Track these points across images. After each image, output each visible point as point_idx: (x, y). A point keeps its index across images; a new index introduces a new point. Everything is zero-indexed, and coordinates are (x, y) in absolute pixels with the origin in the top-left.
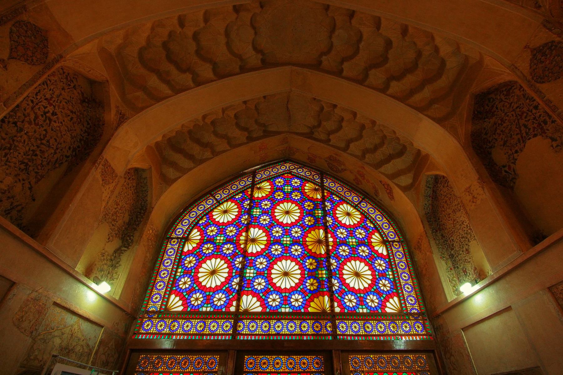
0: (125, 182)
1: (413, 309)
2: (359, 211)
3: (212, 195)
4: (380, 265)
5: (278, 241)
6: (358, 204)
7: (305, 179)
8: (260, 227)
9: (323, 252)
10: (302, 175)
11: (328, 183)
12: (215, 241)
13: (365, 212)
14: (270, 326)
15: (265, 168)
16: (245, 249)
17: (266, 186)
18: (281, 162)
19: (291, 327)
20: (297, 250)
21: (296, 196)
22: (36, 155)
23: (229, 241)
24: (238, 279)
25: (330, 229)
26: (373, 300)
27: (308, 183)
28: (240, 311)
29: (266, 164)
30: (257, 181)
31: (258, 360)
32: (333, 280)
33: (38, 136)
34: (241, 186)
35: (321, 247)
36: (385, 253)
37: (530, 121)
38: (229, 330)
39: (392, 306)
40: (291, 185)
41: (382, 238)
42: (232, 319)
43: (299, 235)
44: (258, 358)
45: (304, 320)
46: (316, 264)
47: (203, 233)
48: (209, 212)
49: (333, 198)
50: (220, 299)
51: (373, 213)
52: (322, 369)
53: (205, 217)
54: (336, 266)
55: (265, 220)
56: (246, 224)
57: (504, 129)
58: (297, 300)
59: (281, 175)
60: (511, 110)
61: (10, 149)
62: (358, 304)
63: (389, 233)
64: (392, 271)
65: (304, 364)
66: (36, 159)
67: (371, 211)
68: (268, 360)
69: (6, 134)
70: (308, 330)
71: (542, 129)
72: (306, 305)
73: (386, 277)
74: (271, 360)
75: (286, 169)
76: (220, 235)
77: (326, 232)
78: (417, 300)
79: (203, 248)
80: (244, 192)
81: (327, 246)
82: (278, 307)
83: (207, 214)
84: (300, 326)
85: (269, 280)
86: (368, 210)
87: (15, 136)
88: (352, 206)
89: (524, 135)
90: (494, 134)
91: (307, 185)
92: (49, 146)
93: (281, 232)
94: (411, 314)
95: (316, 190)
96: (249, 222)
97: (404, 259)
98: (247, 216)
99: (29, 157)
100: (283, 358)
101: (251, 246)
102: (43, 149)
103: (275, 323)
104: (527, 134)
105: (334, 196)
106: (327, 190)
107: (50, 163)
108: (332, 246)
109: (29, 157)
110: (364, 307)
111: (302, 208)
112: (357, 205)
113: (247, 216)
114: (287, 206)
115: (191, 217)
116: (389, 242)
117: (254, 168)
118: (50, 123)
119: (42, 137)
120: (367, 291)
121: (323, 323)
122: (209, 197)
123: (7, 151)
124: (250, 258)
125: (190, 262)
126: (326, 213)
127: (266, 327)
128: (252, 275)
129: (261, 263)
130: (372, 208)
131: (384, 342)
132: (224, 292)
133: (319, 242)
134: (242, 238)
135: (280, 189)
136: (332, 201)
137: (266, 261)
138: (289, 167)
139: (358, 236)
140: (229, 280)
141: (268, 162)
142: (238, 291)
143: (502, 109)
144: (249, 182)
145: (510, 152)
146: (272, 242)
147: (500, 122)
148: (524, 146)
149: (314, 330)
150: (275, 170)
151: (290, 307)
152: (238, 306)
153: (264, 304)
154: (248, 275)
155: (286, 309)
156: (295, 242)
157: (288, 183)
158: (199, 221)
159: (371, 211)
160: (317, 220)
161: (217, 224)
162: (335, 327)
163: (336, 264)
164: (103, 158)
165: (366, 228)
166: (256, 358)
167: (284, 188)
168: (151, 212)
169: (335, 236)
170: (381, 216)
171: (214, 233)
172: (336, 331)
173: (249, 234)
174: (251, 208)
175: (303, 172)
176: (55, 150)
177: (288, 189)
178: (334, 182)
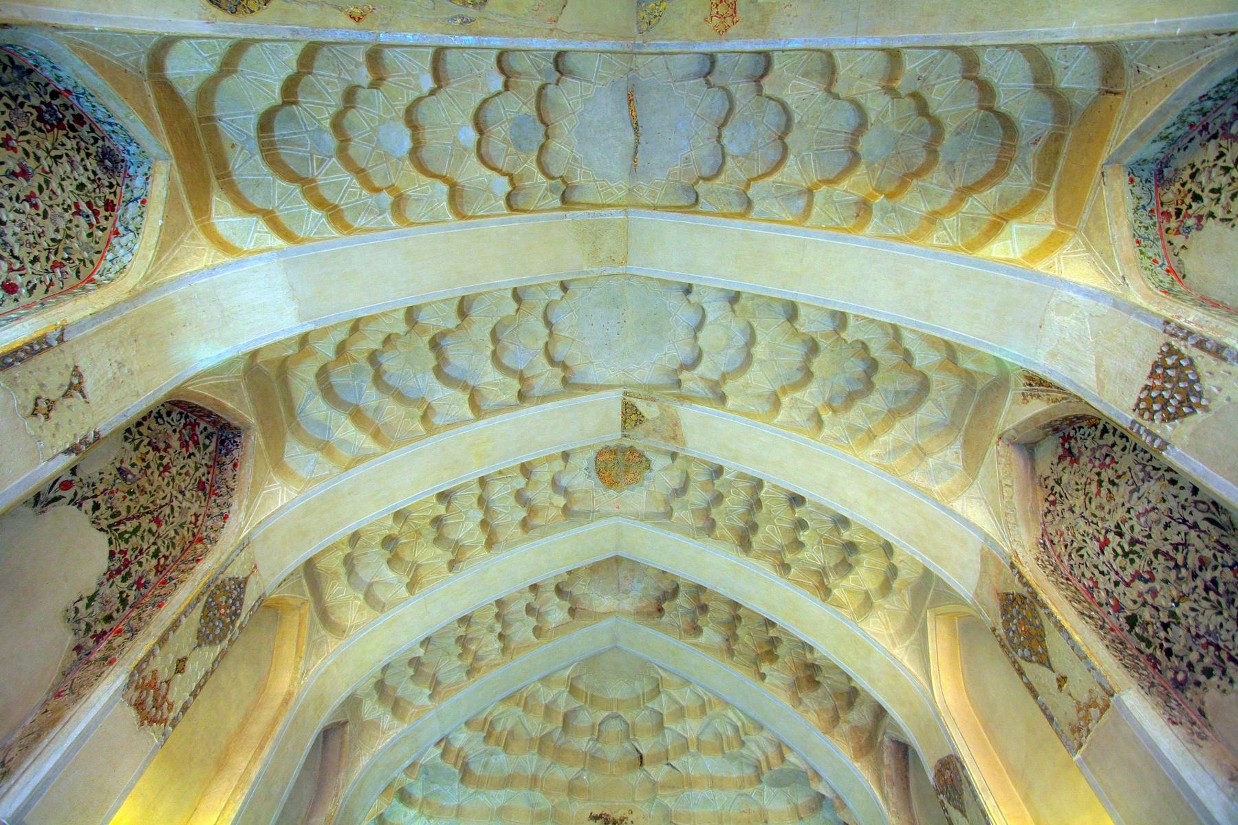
22: (1214, 581)
33: (1173, 574)
37: (140, 542)
57: (149, 472)
60: (175, 493)
61: (1218, 648)
66: (1225, 584)
69: (1191, 649)
71: (118, 571)
87: (1189, 631)
89: (122, 528)
90: (149, 444)
92: (1185, 545)
99: (1223, 601)
102: (1198, 564)
104: (121, 535)
107: (1225, 541)
109: (1223, 601)
118: (1138, 541)
119: (1171, 564)
123: (1224, 656)
143: (184, 471)
145: (101, 487)
147: (165, 461)
148: (101, 530)
164: (1133, 422)
176: (1190, 527)
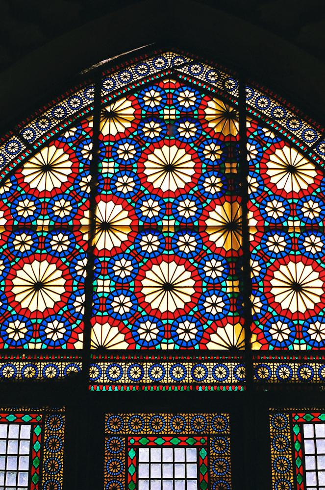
5: (152, 227)
6: (313, 147)
7: (205, 91)
8: (118, 199)
11: (255, 99)
14: (142, 372)
19: (178, 372)
21: (188, 130)
23: (60, 227)
24: (84, 296)
25: (253, 201)
28: (92, 348)
31: (126, 419)
34: (73, 109)
40: (176, 105)
43: (192, 214)
44: (126, 416)
45: (199, 363)
48: (15, 169)
50: (56, 331)
52: (227, 431)
53: (9, 181)
55: (126, 184)
65: (199, 424)
68: (141, 419)
70: (205, 377)
74: (147, 419)
76: (41, 217)
80: (78, 121)
85: (138, 298)
88: (300, 151)
91: (210, 104)
93: (158, 209)
103: (152, 368)
108: (254, 235)
112: (310, 150)
114: (169, 153)
121: (231, 366)
124: (101, 259)
128: (107, 290)
135: (154, 116)
136: (260, 141)
137: (132, 265)
138: (172, 61)
140: (68, 298)
144: (90, 99)
152: (87, 341)
153: (131, 336)
154: (100, 289)
157: (170, 100)
161: (33, 194)
163: (259, 269)
166: (123, 416)
177: (170, 113)
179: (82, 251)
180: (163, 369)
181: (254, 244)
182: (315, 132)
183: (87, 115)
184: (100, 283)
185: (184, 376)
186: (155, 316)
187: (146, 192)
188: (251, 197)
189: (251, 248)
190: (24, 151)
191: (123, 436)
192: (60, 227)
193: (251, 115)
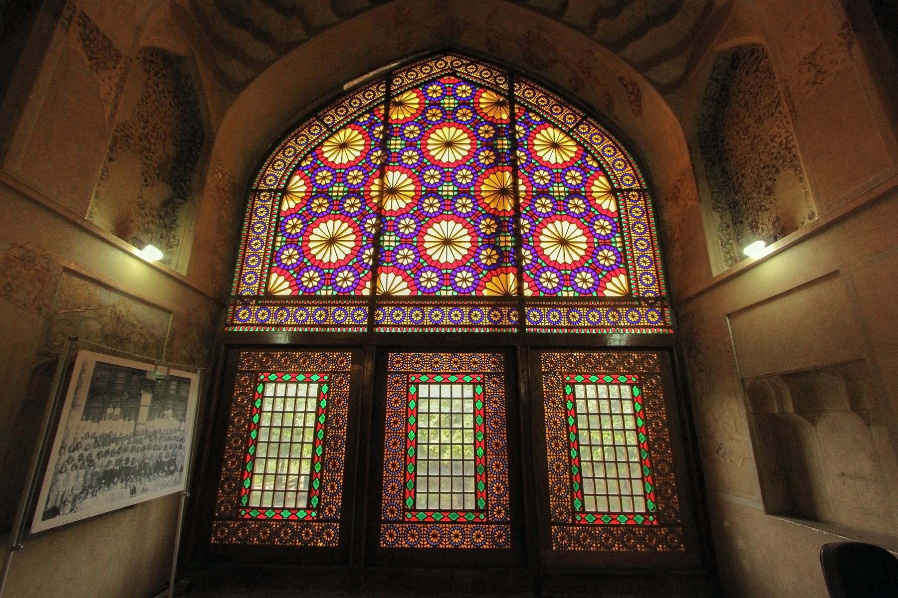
0: (149, 79)
1: (648, 291)
2: (575, 140)
3: (318, 119)
4: (603, 227)
5: (432, 192)
8: (404, 168)
9: (509, 208)
10: (476, 78)
12: (330, 194)
13: (585, 141)
15: (407, 66)
16: (379, 205)
17: (412, 99)
18: (436, 53)
20: (465, 205)
21: (463, 114)
23: (353, 192)
24: (372, 250)
25: (523, 171)
26: (584, 280)
27: (485, 91)
29: (410, 58)
30: (394, 91)
32: (523, 250)
35: (506, 201)
36: (613, 209)
38: (363, 320)
39: (616, 286)
40: (455, 96)
41: (611, 184)
42: (365, 305)
43: (469, 181)
45: (476, 307)
46: (496, 226)
47: (311, 181)
48: (316, 146)
49: (530, 117)
50: (345, 278)
51: (599, 144)
53: (310, 155)
54: (530, 229)
55: (411, 157)
56: (380, 165)
58: (464, 279)
59: (437, 77)
62: (561, 285)
63: (623, 176)
64: (622, 237)
65: (475, 363)
67: (597, 139)
68: (422, 358)
70: (481, 320)
72: (478, 285)
73: (610, 246)
75: (445, 66)
76: (337, 184)
77: (515, 176)
78: (656, 279)
79: (313, 205)
81: (516, 198)
82: (436, 289)
83: (313, 150)
84: (470, 314)
85: (420, 252)
86: (591, 138)
91: (484, 95)
94: (644, 299)
95: (498, 104)
96: (383, 161)
97: (644, 218)
98: (380, 152)
100: (445, 356)
101: (389, 201)
103: (432, 311)
105: (531, 115)
106: (519, 103)
108: (524, 198)
110: (570, 289)
111: (474, 136)
112: (571, 130)
113: (380, 152)
115: (288, 157)
116: (620, 190)
117: (388, 67)
120: (577, 267)
121: (505, 310)
122: (314, 121)
125: (294, 226)
126: (515, 145)
127: (417, 315)
128: (392, 244)
129: (407, 226)
130: (599, 134)
131: (597, 335)
132: (350, 269)
133: (503, 192)
134: (373, 188)
135: (436, 104)
136: (527, 123)
138: (452, 63)
139: (569, 182)
140: (358, 251)
141: (413, 53)
142: (372, 267)
144: (380, 92)
146: (423, 193)
149: (491, 320)
150: (426, 70)
151: (454, 289)
152: (374, 288)
153: (415, 284)
154: (386, 244)
155: (447, 292)
156: (463, 192)
158: (300, 162)
159: (597, 139)
160: (499, 156)
161: (331, 167)
162: (523, 316)
163: (529, 226)
165: (584, 169)
167: (442, 101)
168: (212, 142)
169: (530, 182)
170: (613, 148)
171: (328, 181)
172: (525, 321)
173: (386, 181)
174: (387, 137)
175: (476, 72)
177: (449, 103)
178: (532, 88)
179: (371, 212)
180: (443, 313)
181: (524, 206)
182: (574, 116)
183: (379, 104)
184: (387, 238)
185: (462, 318)
186: (435, 267)
187: (429, 164)
188: (521, 167)
189: (521, 209)
190: (325, 133)
191: (405, 373)
192: (353, 192)
193: (519, 103)
